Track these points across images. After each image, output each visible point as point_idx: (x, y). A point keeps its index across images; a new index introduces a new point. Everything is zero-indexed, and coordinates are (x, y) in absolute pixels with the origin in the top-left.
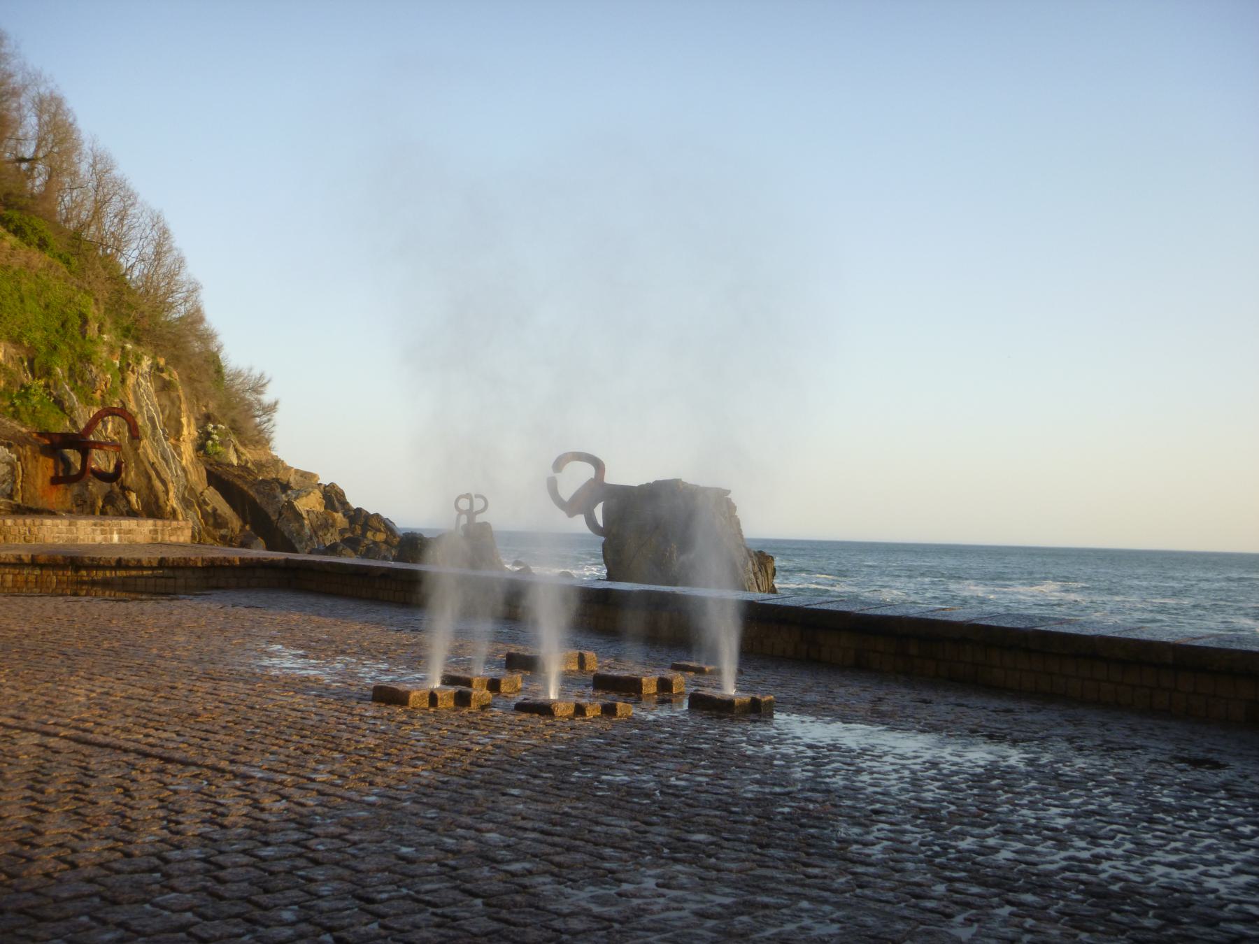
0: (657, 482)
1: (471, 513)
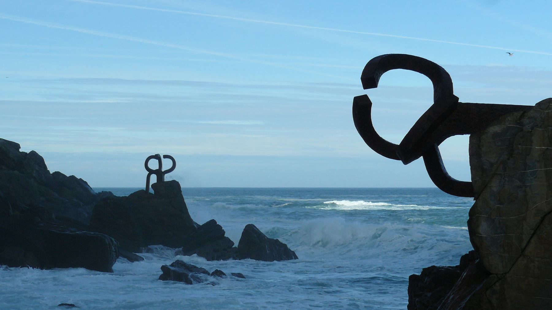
1: (160, 173)
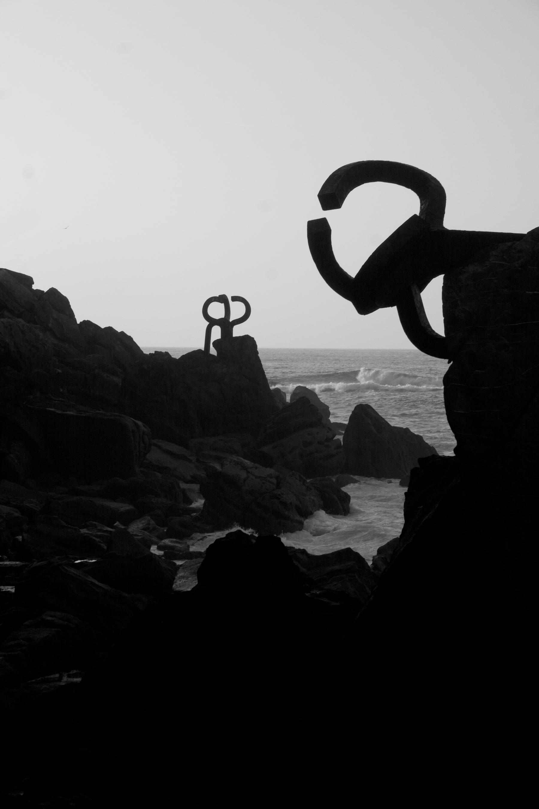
1: (226, 324)
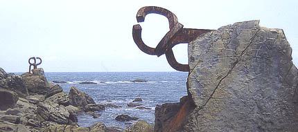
0: (237, 25)
